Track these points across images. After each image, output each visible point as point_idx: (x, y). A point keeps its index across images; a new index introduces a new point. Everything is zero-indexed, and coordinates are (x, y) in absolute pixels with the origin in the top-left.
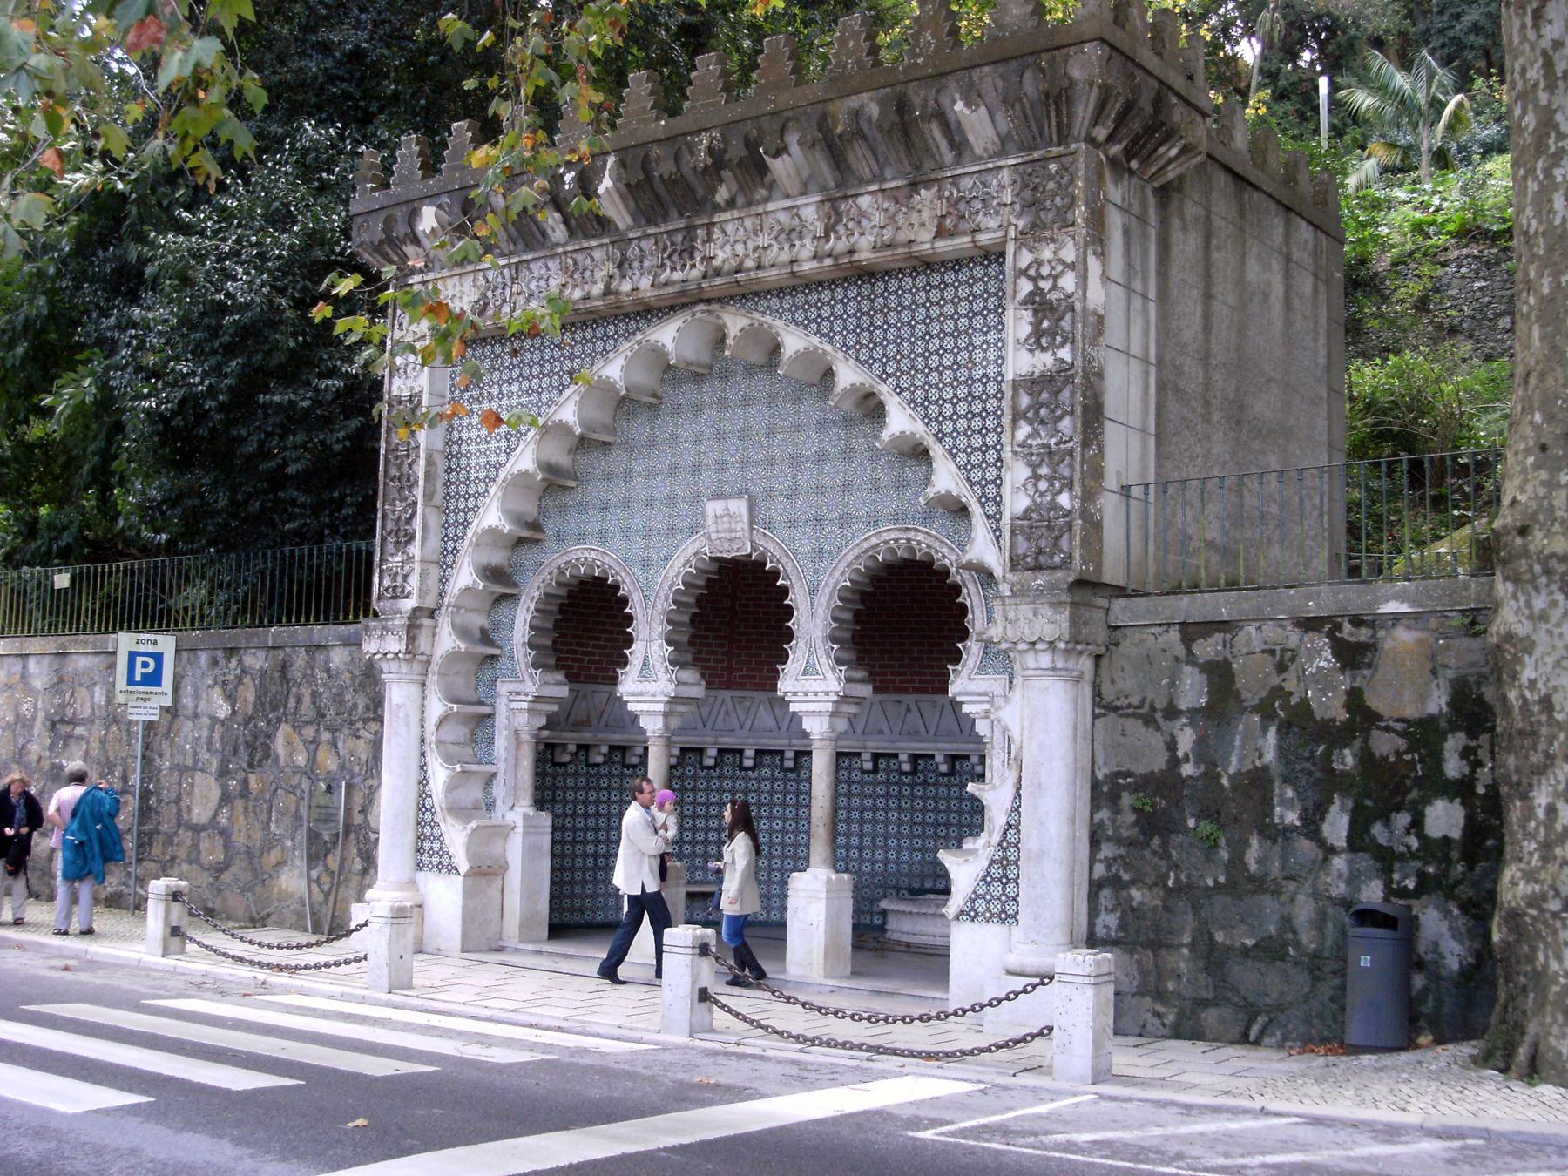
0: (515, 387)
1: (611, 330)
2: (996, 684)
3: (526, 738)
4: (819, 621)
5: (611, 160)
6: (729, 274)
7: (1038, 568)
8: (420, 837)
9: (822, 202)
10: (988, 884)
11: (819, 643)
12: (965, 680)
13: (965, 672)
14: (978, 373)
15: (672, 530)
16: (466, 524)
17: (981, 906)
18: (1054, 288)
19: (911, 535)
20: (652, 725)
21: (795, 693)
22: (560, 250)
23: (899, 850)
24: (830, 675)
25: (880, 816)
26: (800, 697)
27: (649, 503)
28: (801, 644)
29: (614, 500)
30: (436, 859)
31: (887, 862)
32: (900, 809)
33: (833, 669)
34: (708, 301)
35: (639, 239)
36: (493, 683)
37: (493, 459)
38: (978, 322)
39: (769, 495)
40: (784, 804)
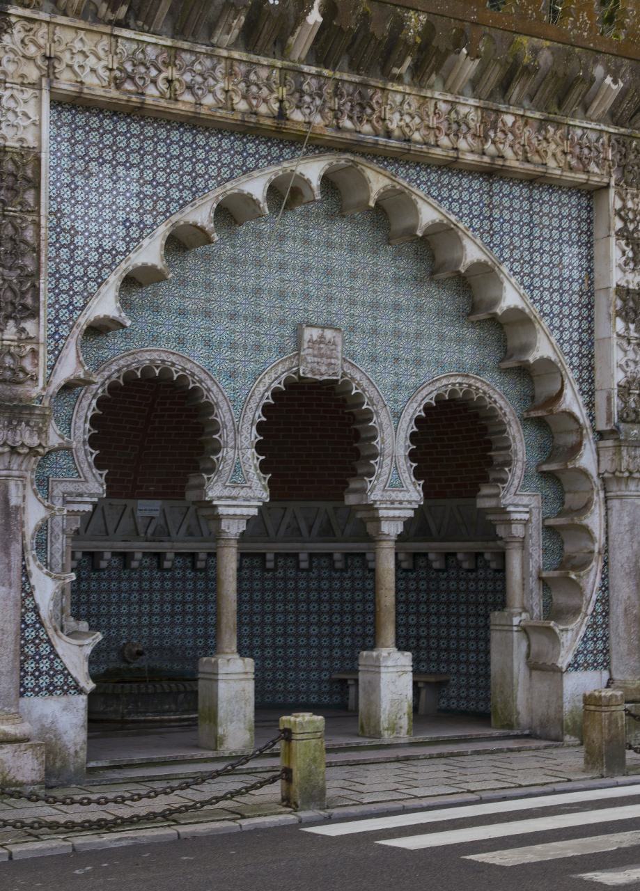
0: (135, 173)
1: (251, 147)
2: (533, 498)
4: (402, 443)
9: (477, 107)
13: (513, 490)
17: (581, 659)
19: (472, 381)
21: (382, 502)
24: (411, 487)
27: (233, 316)
28: (388, 461)
29: (189, 305)
30: (44, 681)
33: (414, 483)
34: (353, 153)
37: (107, 244)
39: (352, 329)
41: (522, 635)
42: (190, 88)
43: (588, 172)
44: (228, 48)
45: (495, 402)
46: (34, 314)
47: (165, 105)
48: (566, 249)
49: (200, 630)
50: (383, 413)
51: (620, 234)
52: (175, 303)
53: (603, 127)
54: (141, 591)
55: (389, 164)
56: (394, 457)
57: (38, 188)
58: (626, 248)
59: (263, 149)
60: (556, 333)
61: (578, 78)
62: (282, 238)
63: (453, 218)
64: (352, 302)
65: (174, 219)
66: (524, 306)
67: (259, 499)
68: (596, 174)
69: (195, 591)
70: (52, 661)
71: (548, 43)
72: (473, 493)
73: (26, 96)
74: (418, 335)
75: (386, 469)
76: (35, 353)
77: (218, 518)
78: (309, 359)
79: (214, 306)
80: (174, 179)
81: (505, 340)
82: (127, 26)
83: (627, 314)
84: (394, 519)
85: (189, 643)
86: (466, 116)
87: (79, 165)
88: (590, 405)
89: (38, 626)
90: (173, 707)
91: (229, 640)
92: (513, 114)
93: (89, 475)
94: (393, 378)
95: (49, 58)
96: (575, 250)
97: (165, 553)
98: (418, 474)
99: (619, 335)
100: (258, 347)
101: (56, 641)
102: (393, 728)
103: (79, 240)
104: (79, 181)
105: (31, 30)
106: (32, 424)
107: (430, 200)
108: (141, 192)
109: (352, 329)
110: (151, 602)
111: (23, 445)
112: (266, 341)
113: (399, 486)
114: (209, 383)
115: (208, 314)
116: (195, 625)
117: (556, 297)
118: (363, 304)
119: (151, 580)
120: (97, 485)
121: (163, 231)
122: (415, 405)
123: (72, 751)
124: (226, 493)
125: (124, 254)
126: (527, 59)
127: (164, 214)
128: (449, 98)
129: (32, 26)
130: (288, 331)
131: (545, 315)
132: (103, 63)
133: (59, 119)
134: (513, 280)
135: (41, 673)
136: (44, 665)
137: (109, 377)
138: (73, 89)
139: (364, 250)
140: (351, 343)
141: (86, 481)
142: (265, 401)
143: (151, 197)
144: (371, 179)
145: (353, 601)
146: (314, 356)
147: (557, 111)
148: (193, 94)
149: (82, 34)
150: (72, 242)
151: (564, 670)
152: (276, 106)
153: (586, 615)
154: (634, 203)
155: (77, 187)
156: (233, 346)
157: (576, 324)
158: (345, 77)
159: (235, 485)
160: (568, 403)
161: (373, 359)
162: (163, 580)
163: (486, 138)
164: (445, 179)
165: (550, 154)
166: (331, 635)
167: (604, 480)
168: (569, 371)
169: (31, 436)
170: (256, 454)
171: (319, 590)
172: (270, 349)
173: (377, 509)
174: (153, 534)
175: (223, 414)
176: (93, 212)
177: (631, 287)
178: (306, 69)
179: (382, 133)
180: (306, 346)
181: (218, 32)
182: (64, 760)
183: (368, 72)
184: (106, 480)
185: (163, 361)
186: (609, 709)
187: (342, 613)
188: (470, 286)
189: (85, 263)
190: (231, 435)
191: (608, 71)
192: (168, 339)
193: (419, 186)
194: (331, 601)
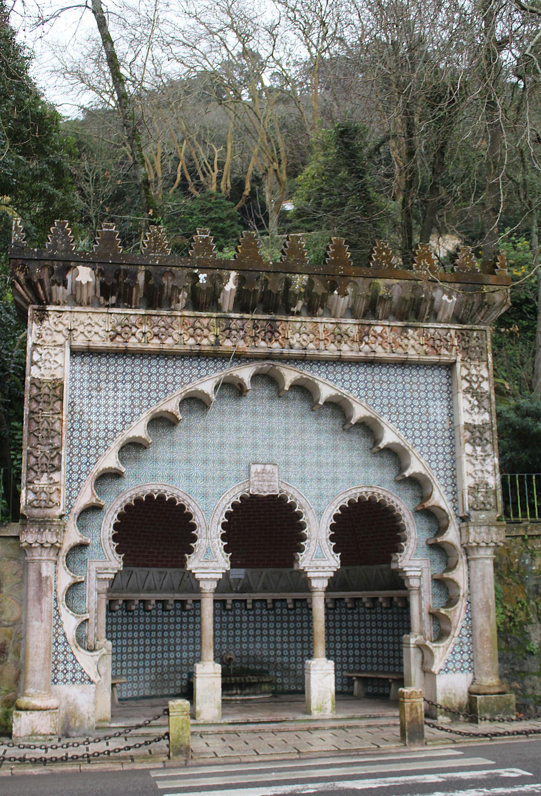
0: (128, 386)
2: (424, 562)
3: (104, 596)
4: (323, 531)
5: (233, 274)
6: (299, 349)
7: (481, 510)
8: (56, 663)
9: (355, 324)
10: (454, 655)
11: (324, 542)
12: (407, 561)
13: (408, 557)
14: (432, 418)
15: (222, 478)
16: (88, 464)
17: (451, 666)
18: (479, 387)
19: (375, 490)
20: (208, 587)
21: (309, 567)
22: (179, 314)
23: (181, 651)
24: (331, 558)
25: (172, 634)
26: (315, 570)
27: (205, 462)
28: (313, 542)
29: (178, 457)
30: (69, 676)
31: (176, 658)
32: (181, 630)
33: (333, 555)
34: (273, 359)
35: (237, 319)
36: (84, 562)
37: (111, 427)
38: (430, 395)
39: (287, 464)
40: (127, 630)
41: (418, 650)
42: (156, 335)
43: (440, 354)
44: (181, 311)
45: (393, 502)
46: (58, 469)
47: (140, 346)
48: (431, 403)
49: (272, 646)
50: (309, 513)
51: (466, 391)
52: (168, 456)
53: (449, 326)
54: (235, 622)
55: (298, 364)
56: (318, 541)
57: (62, 400)
58: (471, 399)
59: (211, 364)
60: (426, 457)
61: (422, 299)
62: (238, 413)
63: (345, 391)
64: (287, 447)
65: (152, 409)
66: (400, 441)
67: (223, 568)
68: (446, 355)
69: (268, 622)
70: (74, 664)
71: (397, 281)
72: (388, 560)
73: (56, 352)
74: (335, 464)
75: (312, 548)
76: (59, 490)
77: (198, 581)
78: (255, 483)
79: (193, 456)
80: (153, 386)
81: (400, 463)
82: (118, 307)
83: (474, 441)
84: (319, 578)
85: (265, 653)
86: (347, 330)
87: (94, 385)
88: (454, 500)
89: (66, 644)
90: (239, 692)
91: (209, 653)
92: (381, 325)
93: (112, 557)
94: (316, 491)
95: (70, 330)
96: (438, 403)
97: (186, 600)
98: (336, 550)
99: (468, 455)
100: (222, 478)
101: (76, 652)
102: (320, 709)
103: (94, 426)
104: (94, 393)
105: (60, 317)
106: (52, 530)
107: (328, 382)
108: (132, 396)
109: (287, 464)
110: (241, 629)
111: (47, 542)
112: (227, 474)
113: (323, 558)
114: (189, 501)
115: (188, 461)
116: (268, 642)
117: (425, 434)
118: (295, 447)
119: (241, 616)
120: (117, 563)
121: (145, 417)
122: (333, 507)
123: (86, 717)
124: (201, 565)
125: (122, 431)
126: (382, 292)
127: (147, 407)
128: (333, 321)
129: (61, 314)
130: (243, 467)
131: (416, 445)
132: (102, 328)
133: (82, 361)
134: (391, 425)
135: (67, 671)
136: (70, 667)
137: (125, 501)
138: (84, 345)
139: (294, 415)
140: (286, 471)
141: (110, 561)
142: (227, 510)
143: (139, 398)
144: (286, 374)
145: (359, 628)
146: (259, 481)
147: (415, 320)
148: (160, 338)
149: (90, 314)
150: (89, 428)
151: (436, 673)
152: (212, 339)
153: (454, 637)
154: (477, 370)
155: (92, 397)
156: (205, 479)
157: (440, 450)
158: (260, 317)
159: (207, 561)
160: (436, 500)
161: (303, 480)
162: (248, 615)
163: (361, 341)
164: (339, 368)
165: (410, 346)
166: (347, 649)
167: (465, 548)
168: (435, 479)
169: (52, 537)
170: (221, 541)
171: (341, 621)
172: (230, 479)
173: (307, 572)
174: (241, 588)
175: (198, 520)
176: (102, 410)
177: (476, 423)
178: (232, 315)
179: (286, 346)
180: (253, 475)
181: (174, 302)
182: (81, 722)
183: (276, 313)
184: (123, 559)
185: (159, 490)
186: (411, 700)
187: (353, 635)
188: (372, 431)
189: (97, 439)
190: (204, 531)
191: (444, 292)
192: (163, 477)
193: (320, 375)
194: (347, 628)
